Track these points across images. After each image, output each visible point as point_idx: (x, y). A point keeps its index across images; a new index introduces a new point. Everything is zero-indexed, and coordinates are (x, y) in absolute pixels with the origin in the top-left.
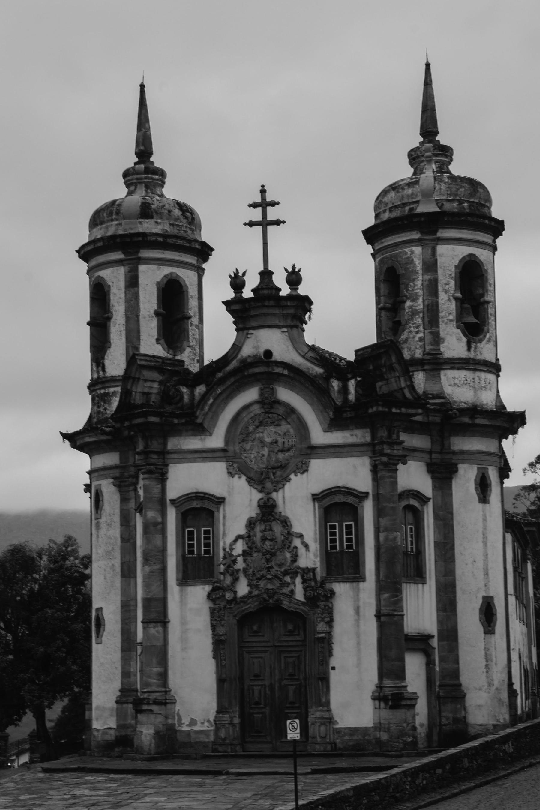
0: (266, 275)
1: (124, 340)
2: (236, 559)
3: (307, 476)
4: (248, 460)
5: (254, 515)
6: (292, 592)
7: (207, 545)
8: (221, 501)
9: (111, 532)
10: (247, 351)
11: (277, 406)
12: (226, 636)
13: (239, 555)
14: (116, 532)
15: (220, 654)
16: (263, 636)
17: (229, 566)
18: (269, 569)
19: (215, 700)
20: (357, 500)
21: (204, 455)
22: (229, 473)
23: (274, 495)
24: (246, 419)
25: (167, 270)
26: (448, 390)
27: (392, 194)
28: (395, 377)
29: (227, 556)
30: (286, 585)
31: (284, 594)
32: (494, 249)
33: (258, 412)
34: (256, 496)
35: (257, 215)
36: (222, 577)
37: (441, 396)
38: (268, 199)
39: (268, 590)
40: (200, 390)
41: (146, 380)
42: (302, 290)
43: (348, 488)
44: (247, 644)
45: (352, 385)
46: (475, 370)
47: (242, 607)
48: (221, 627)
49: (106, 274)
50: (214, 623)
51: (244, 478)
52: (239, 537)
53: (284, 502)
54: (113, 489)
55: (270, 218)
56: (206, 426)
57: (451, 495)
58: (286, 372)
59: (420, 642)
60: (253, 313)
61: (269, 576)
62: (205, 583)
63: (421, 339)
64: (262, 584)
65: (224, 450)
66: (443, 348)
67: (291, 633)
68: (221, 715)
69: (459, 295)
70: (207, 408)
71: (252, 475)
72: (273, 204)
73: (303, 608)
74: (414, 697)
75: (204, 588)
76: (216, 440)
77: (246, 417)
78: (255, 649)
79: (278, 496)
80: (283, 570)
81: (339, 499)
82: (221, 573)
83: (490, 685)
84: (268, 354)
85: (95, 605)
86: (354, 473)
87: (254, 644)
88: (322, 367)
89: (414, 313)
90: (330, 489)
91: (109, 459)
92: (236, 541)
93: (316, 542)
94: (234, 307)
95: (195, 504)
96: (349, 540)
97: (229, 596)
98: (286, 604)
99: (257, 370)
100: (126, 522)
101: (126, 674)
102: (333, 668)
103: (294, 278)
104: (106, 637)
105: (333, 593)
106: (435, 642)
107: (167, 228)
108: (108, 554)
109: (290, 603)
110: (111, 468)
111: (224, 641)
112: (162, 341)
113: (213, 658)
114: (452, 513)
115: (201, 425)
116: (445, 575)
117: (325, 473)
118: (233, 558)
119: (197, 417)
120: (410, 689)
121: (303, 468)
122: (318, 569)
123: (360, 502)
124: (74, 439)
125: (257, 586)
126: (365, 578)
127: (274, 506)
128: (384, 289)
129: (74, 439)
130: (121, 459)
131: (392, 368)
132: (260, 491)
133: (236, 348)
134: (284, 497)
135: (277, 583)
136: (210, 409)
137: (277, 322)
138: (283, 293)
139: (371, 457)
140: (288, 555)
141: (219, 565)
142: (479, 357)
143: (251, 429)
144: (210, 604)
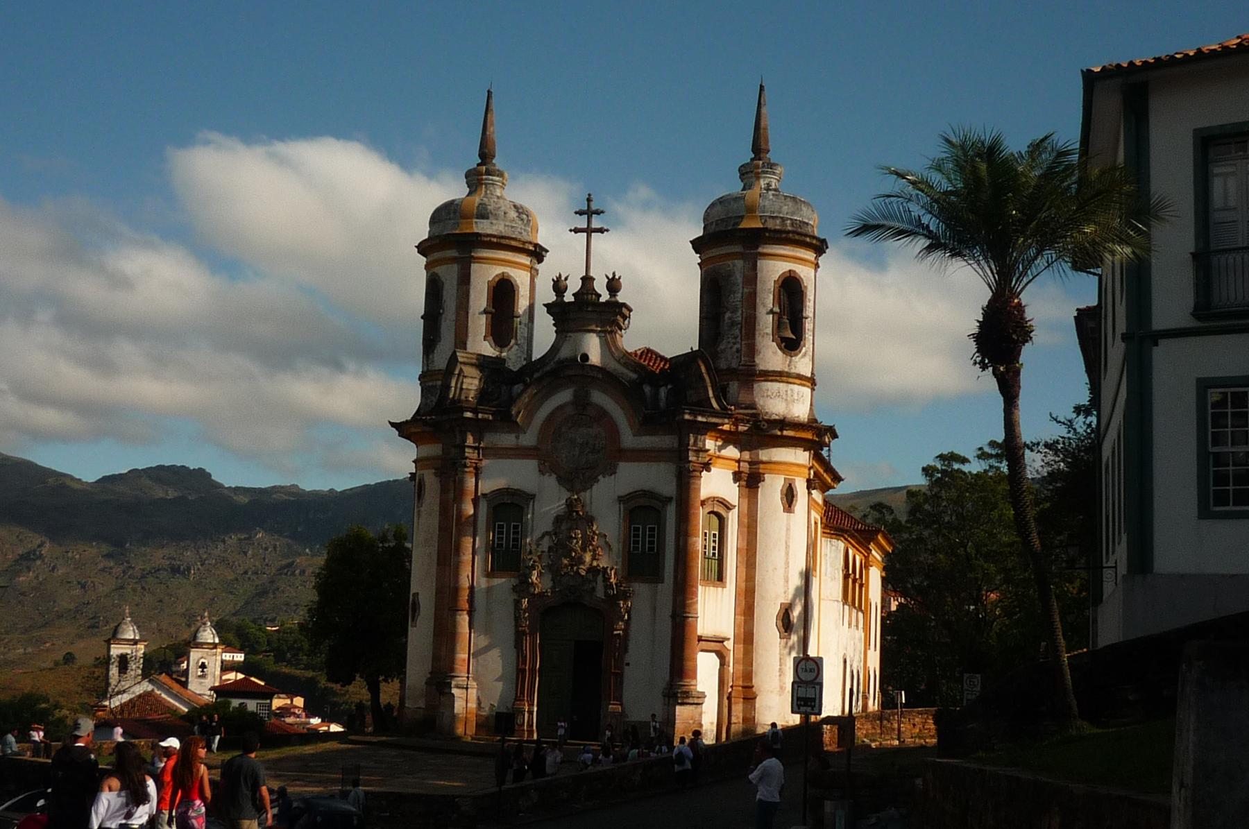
0: (587, 280)
1: (453, 336)
6: (594, 589)
7: (515, 540)
8: (532, 497)
10: (565, 353)
14: (435, 521)
18: (572, 566)
25: (496, 271)
26: (760, 402)
27: (719, 207)
32: (817, 266)
34: (566, 495)
37: (752, 406)
38: (594, 207)
40: (518, 388)
42: (621, 298)
45: (663, 392)
49: (440, 270)
51: (554, 476)
52: (547, 533)
55: (595, 225)
58: (600, 376)
59: (716, 645)
63: (738, 351)
65: (535, 448)
66: (757, 361)
69: (777, 309)
72: (598, 213)
74: (702, 696)
76: (529, 439)
81: (642, 502)
83: (782, 688)
84: (585, 357)
85: (413, 591)
86: (657, 477)
88: (635, 371)
89: (733, 324)
91: (434, 450)
92: (543, 536)
95: (507, 500)
96: (651, 542)
101: (436, 658)
102: (628, 664)
103: (613, 285)
106: (729, 645)
107: (501, 228)
112: (490, 338)
117: (631, 477)
120: (700, 688)
124: (403, 429)
129: (403, 429)
133: (555, 348)
137: (593, 327)
138: (602, 300)
142: (793, 371)
143: (564, 429)
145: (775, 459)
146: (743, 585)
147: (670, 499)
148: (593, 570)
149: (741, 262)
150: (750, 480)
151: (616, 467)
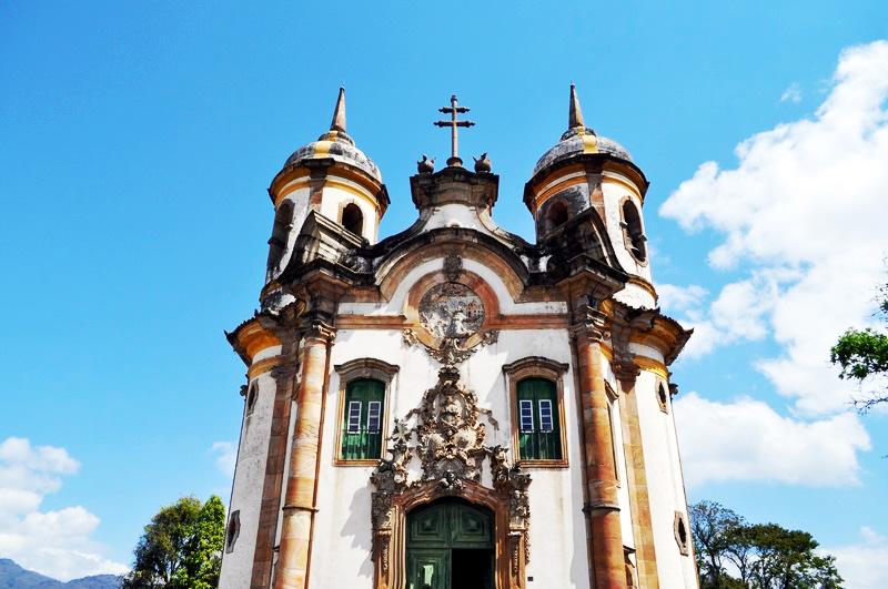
2: (410, 434)
4: (428, 329)
5: (433, 386)
8: (395, 369)
9: (259, 427)
10: (431, 225)
11: (463, 276)
12: (390, 532)
13: (413, 430)
14: (267, 425)
16: (437, 535)
17: (401, 441)
18: (450, 447)
20: (555, 374)
21: (379, 322)
22: (406, 341)
23: (457, 365)
24: (428, 289)
28: (595, 248)
29: (400, 429)
31: (467, 480)
33: (442, 281)
35: (447, 118)
36: (389, 457)
41: (322, 242)
43: (545, 359)
44: (416, 545)
46: (644, 287)
50: (377, 512)
54: (272, 381)
56: (383, 290)
57: (635, 398)
60: (441, 188)
61: (450, 457)
62: (367, 464)
64: (440, 466)
70: (386, 271)
71: (432, 344)
72: (462, 110)
73: (492, 498)
77: (428, 286)
78: (425, 552)
79: (463, 369)
80: (466, 450)
82: (390, 451)
87: (425, 546)
90: (525, 359)
91: (272, 351)
92: (409, 416)
94: (421, 182)
95: (365, 373)
97: (398, 478)
98: (468, 494)
99: (443, 238)
100: (280, 413)
102: (530, 579)
104: (239, 543)
105: (529, 481)
108: (255, 449)
110: (271, 359)
111: (389, 536)
114: (637, 417)
115: (378, 287)
116: (636, 483)
117: (516, 344)
118: (406, 432)
119: (375, 280)
121: (490, 338)
122: (509, 452)
123: (559, 376)
125: (433, 469)
127: (456, 376)
128: (548, 224)
130: (282, 351)
131: (592, 238)
132: (441, 362)
133: (421, 223)
134: (469, 370)
135: (459, 465)
136: (389, 274)
139: (569, 330)
140: (475, 433)
141: (388, 439)
143: (433, 297)
145: (643, 354)
146: (633, 487)
147: (565, 367)
148: (479, 455)
149: (586, 185)
150: (627, 373)
151: (496, 336)
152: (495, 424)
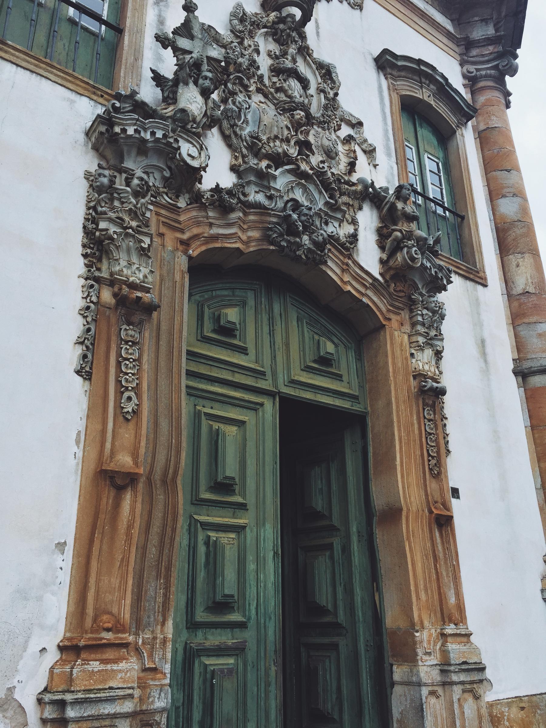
3: (361, 18)
15: (119, 364)
16: (244, 351)
19: (65, 577)
30: (339, 216)
31: (333, 239)
39: (296, 205)
47: (211, 225)
48: (135, 259)
53: (318, 33)
61: (304, 167)
67: (324, 363)
68: (95, 666)
73: (375, 299)
75: (72, 102)
81: (425, 94)
87: (215, 373)
90: (420, 62)
93: (389, 155)
98: (333, 269)
109: (343, 270)
113: (78, 372)
126: (486, 279)
144: (90, 163)
152: (370, 152)
